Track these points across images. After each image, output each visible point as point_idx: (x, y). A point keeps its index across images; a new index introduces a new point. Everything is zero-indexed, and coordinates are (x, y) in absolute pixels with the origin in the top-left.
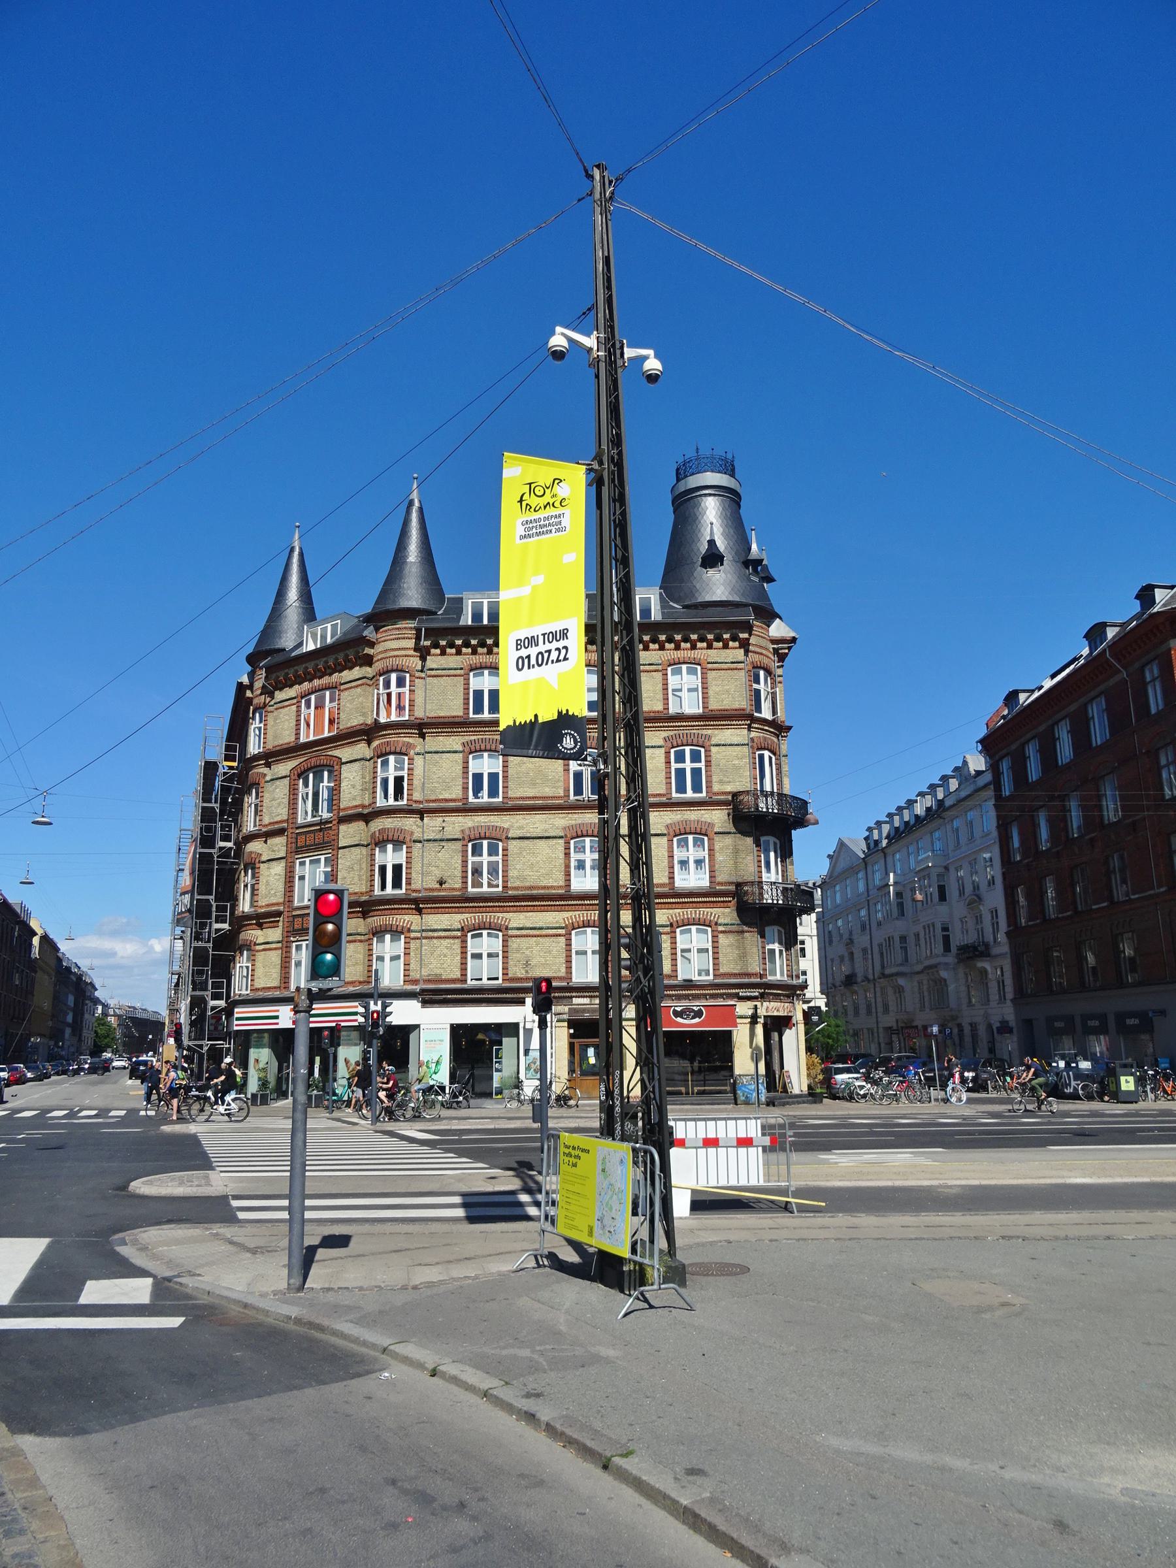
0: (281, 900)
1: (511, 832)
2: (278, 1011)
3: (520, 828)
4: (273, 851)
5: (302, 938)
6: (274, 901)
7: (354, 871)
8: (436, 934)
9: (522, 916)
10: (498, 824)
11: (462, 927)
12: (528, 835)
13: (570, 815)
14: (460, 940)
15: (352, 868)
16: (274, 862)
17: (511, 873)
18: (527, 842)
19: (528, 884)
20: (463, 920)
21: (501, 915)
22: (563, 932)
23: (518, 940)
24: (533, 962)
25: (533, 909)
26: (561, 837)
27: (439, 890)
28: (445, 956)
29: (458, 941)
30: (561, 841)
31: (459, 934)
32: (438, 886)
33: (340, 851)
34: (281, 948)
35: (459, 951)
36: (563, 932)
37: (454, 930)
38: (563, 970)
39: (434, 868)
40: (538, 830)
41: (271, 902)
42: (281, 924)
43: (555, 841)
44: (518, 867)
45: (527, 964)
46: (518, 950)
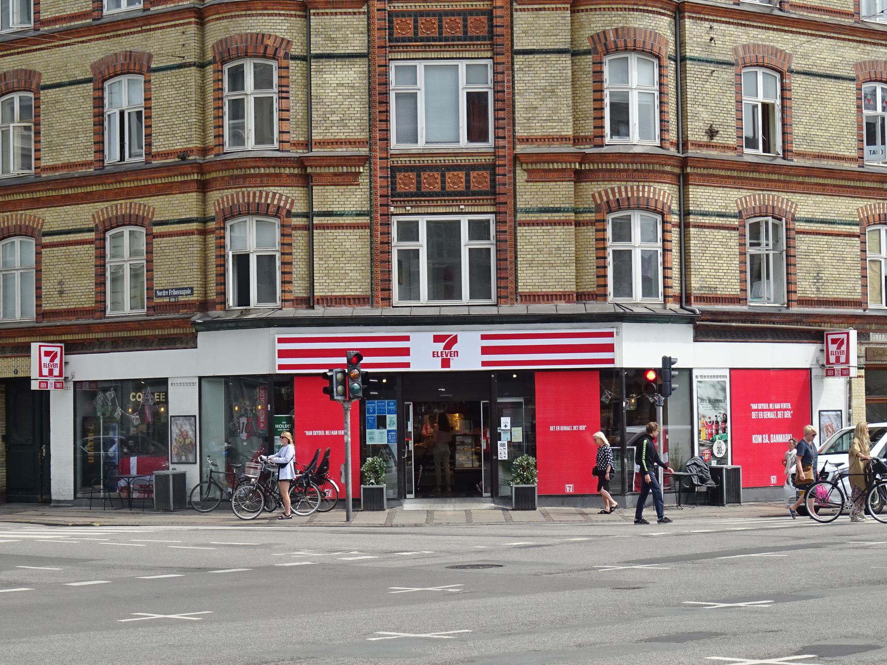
0: (364, 136)
1: (794, 60)
2: (407, 339)
3: (805, 56)
4: (331, 39)
5: (420, 210)
6: (342, 136)
7: (557, 96)
8: (707, 220)
9: (811, 199)
10: (779, 46)
11: (740, 212)
12: (815, 70)
13: (862, 46)
14: (737, 232)
15: (553, 91)
16: (332, 62)
17: (797, 130)
18: (814, 80)
19: (816, 150)
20: (741, 199)
21: (785, 196)
22: (856, 229)
23: (807, 238)
24: (825, 275)
25: (823, 190)
26: (852, 80)
27: (708, 146)
28: (720, 258)
29: (735, 234)
30: (852, 85)
31: (735, 222)
32: (705, 139)
33: (518, 59)
34: (369, 226)
35: (737, 251)
36: (856, 229)
37: (731, 216)
38: (859, 289)
39: (700, 109)
40: (826, 64)
41: (329, 136)
42: (364, 180)
43: (846, 84)
44: (804, 120)
45: (818, 278)
46: (807, 255)
